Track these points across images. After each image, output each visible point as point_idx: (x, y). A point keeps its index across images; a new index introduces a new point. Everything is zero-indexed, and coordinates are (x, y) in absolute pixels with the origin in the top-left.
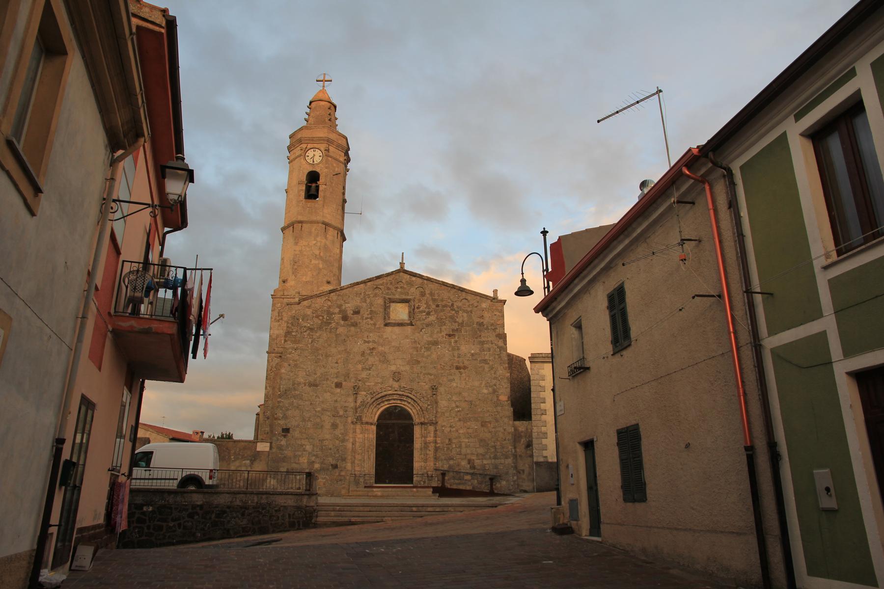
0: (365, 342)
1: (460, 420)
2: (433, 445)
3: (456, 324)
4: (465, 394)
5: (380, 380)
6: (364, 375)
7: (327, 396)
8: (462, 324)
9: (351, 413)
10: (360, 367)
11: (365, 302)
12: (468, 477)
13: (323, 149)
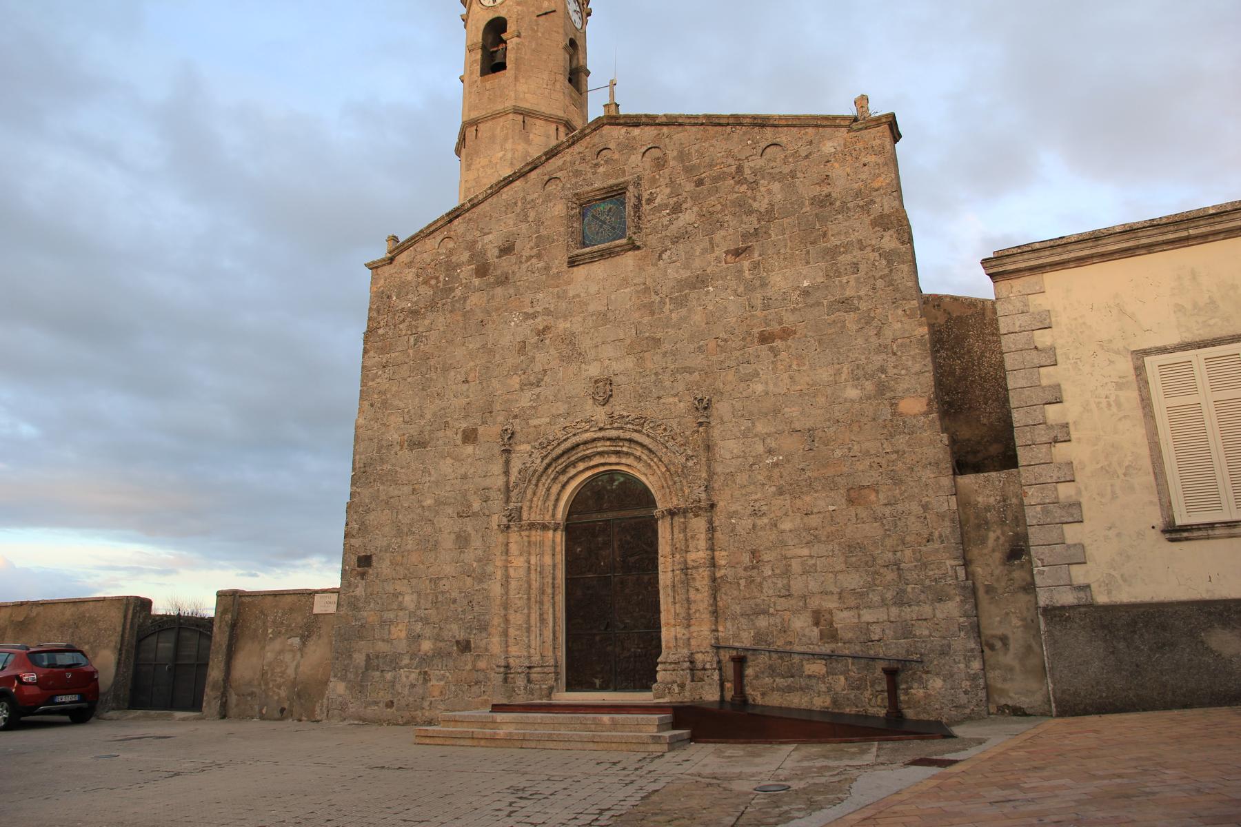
0: (527, 316)
1: (780, 491)
2: (705, 572)
3: (754, 218)
4: (792, 411)
5: (563, 408)
6: (525, 400)
7: (447, 466)
8: (769, 215)
9: (497, 504)
10: (515, 381)
12: (817, 668)
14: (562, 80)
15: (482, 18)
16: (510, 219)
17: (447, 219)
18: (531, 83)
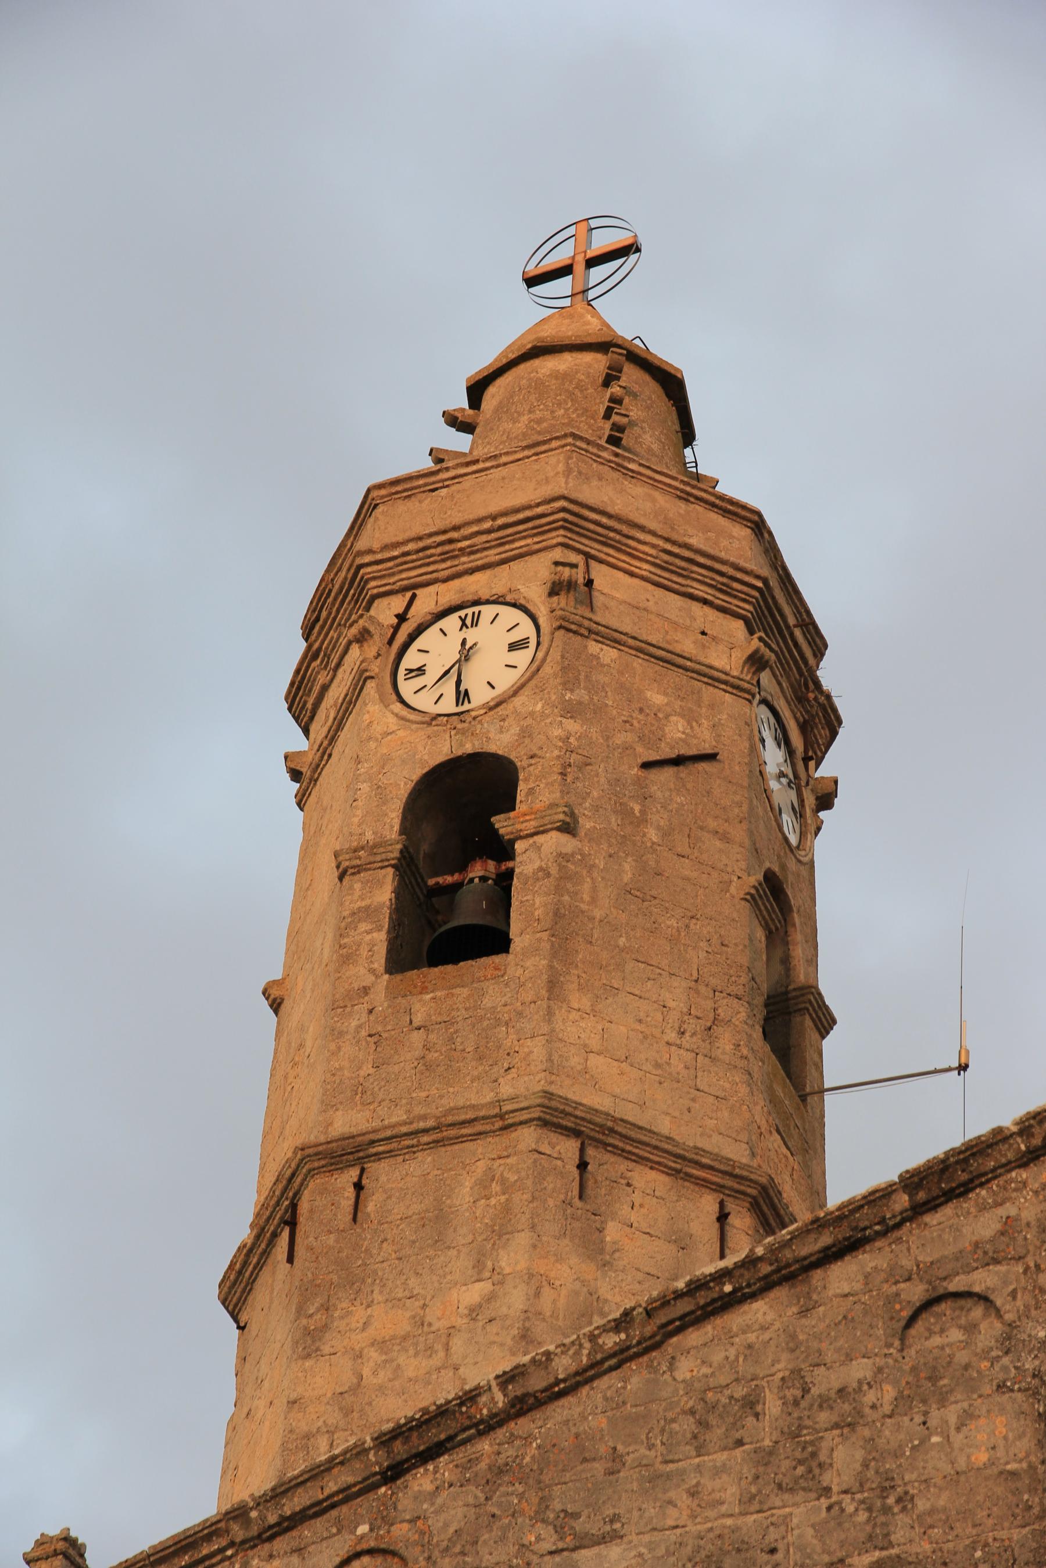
11: (809, 1472)
13: (535, 594)
14: (740, 1027)
15: (392, 752)
16: (724, 1477)
17: (378, 1461)
18: (598, 1018)
